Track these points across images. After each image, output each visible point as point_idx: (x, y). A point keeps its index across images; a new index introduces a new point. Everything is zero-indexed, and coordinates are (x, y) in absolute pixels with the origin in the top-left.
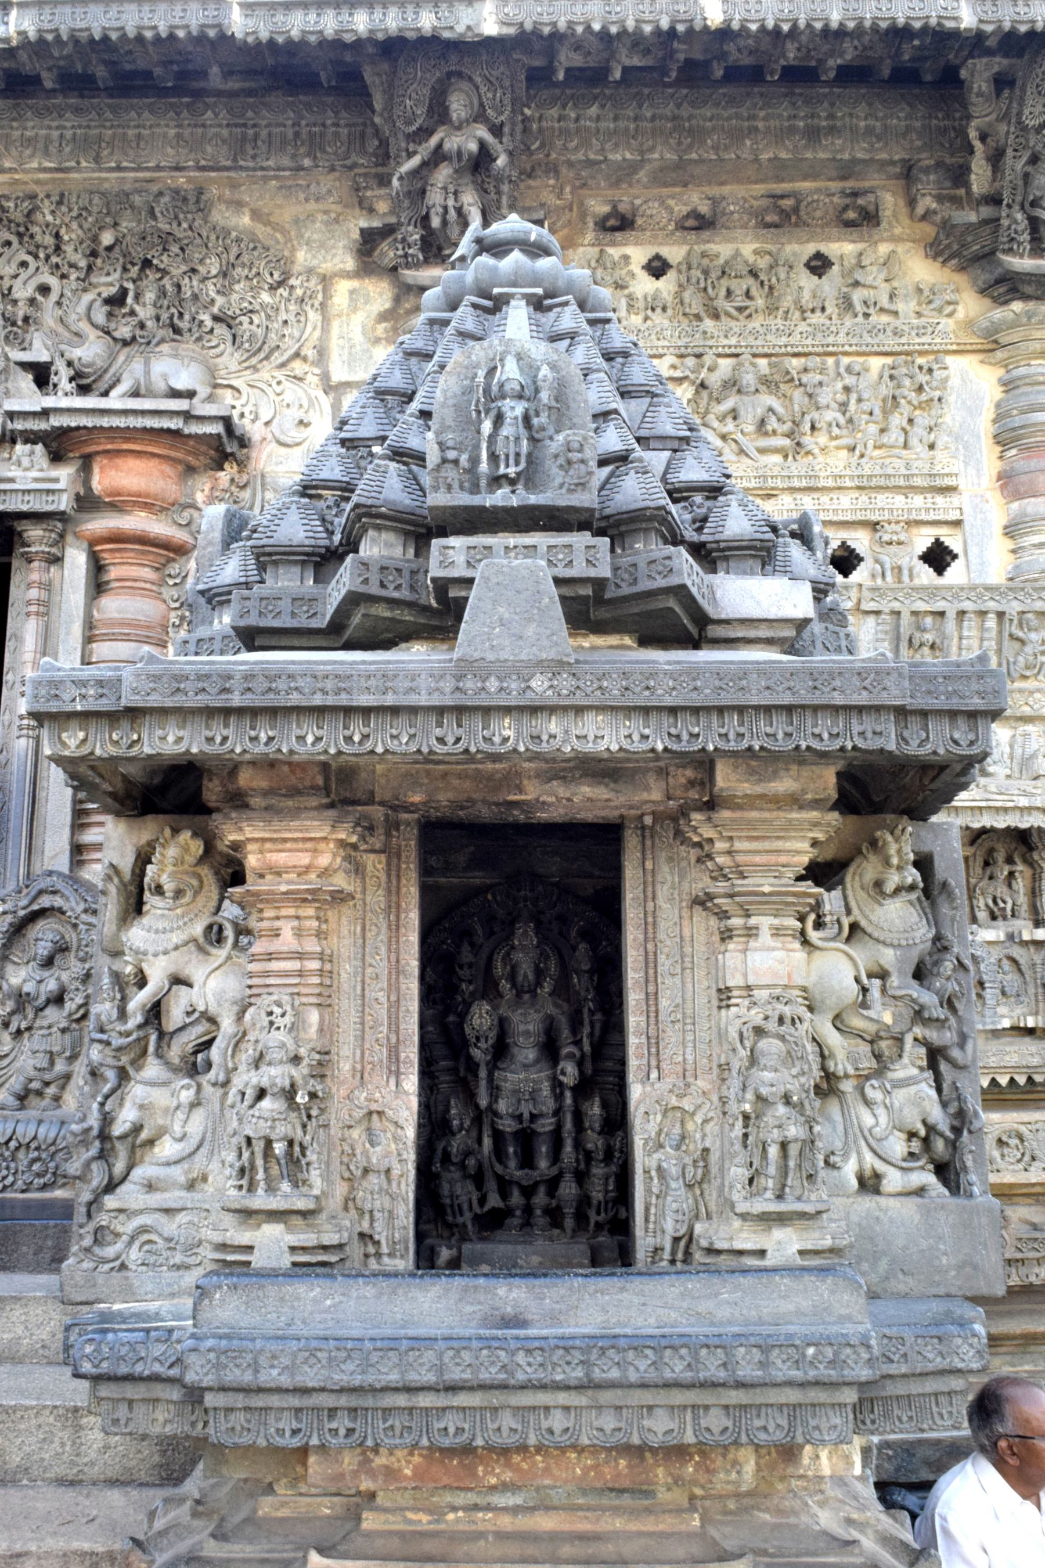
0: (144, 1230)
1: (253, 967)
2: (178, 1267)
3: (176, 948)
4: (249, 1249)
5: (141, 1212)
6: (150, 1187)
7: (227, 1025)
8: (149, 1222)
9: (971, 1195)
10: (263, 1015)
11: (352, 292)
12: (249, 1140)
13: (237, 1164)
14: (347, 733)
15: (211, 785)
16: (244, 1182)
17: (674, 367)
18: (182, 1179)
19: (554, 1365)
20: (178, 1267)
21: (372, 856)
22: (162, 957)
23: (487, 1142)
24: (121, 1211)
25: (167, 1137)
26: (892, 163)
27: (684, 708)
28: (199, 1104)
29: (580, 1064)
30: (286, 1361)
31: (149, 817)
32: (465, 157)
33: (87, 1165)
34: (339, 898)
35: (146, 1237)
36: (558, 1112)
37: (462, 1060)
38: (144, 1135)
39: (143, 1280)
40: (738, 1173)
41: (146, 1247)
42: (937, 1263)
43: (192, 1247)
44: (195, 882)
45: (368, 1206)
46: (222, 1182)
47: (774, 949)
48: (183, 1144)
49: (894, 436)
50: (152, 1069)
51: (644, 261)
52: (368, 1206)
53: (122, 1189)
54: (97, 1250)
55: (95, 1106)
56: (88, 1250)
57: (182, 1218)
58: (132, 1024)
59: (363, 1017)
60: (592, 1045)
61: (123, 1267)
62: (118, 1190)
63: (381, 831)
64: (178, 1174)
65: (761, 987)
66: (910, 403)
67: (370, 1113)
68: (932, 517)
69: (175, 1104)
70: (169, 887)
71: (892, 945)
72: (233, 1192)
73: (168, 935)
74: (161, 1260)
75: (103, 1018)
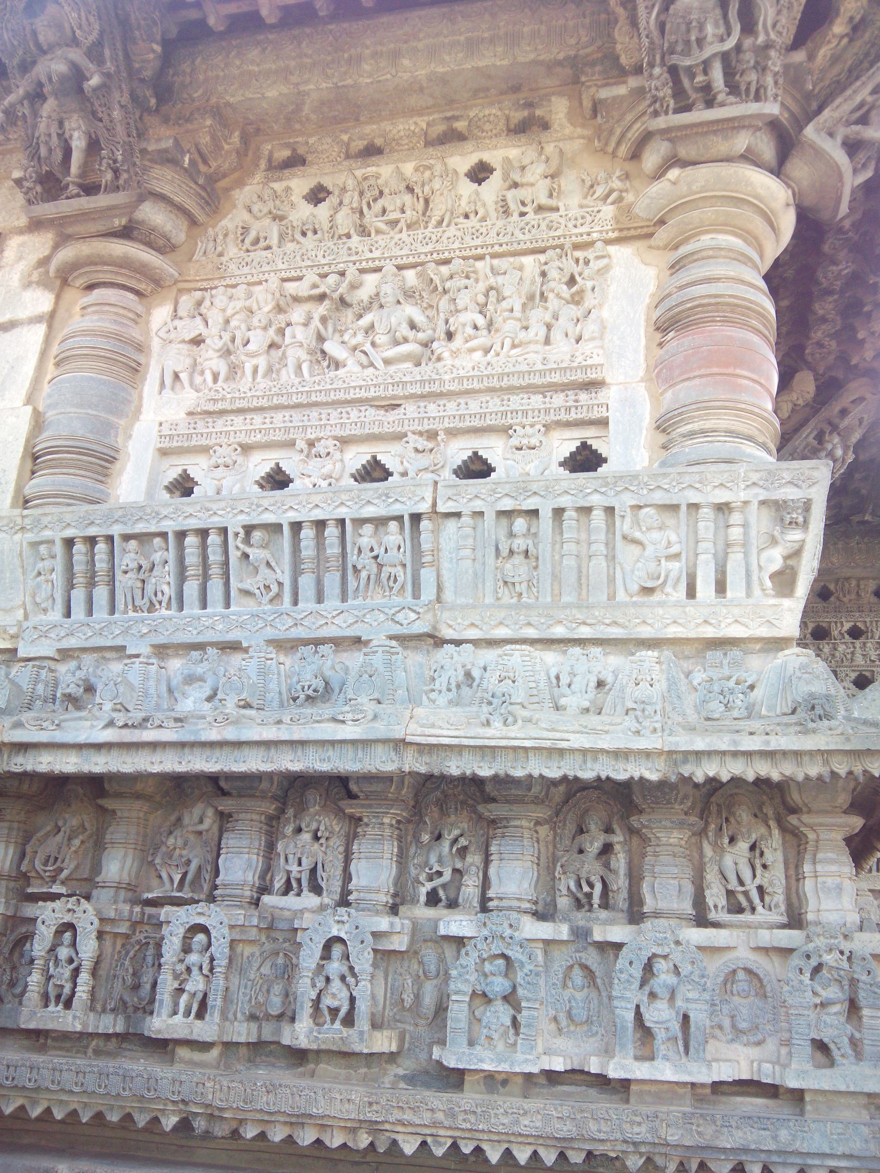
11: (22, 245)
17: (315, 286)
26: (559, 63)
32: (55, 79)
49: (537, 331)
51: (306, 191)
66: (558, 296)
68: (573, 416)
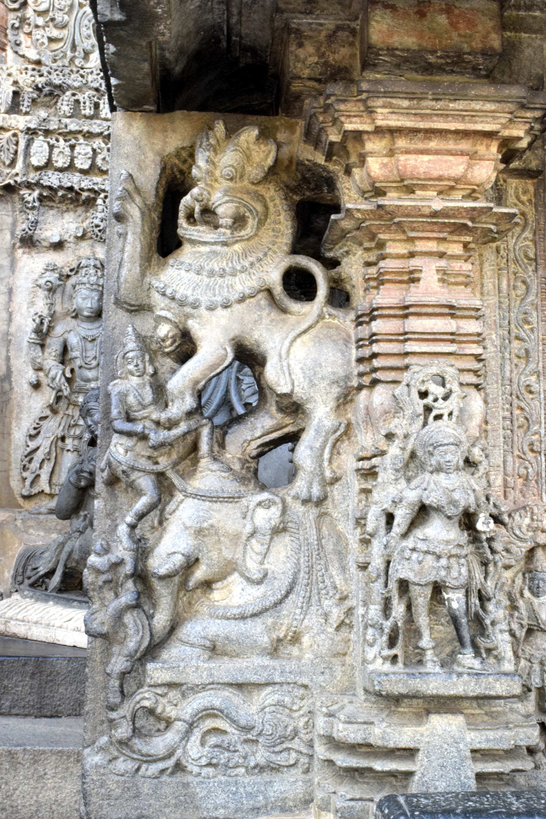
0: (210, 713)
2: (260, 769)
3: (242, 300)
4: (410, 753)
5: (204, 687)
6: (214, 650)
7: (321, 414)
8: (217, 703)
10: (415, 395)
12: (404, 586)
13: (388, 624)
15: (301, 53)
18: (265, 640)
20: (260, 769)
22: (220, 312)
24: (171, 685)
25: (235, 576)
28: (285, 530)
31: (178, 114)
33: (119, 617)
35: (209, 724)
38: (200, 573)
41: (213, 740)
43: (284, 738)
44: (259, 207)
48: (262, 588)
50: (209, 476)
53: (173, 652)
54: (137, 743)
55: (123, 529)
56: (123, 743)
57: (267, 697)
58: (176, 410)
61: (179, 767)
62: (165, 655)
64: (258, 631)
69: (248, 529)
70: (225, 210)
72: (380, 666)
73: (228, 280)
74: (236, 759)
75: (131, 399)
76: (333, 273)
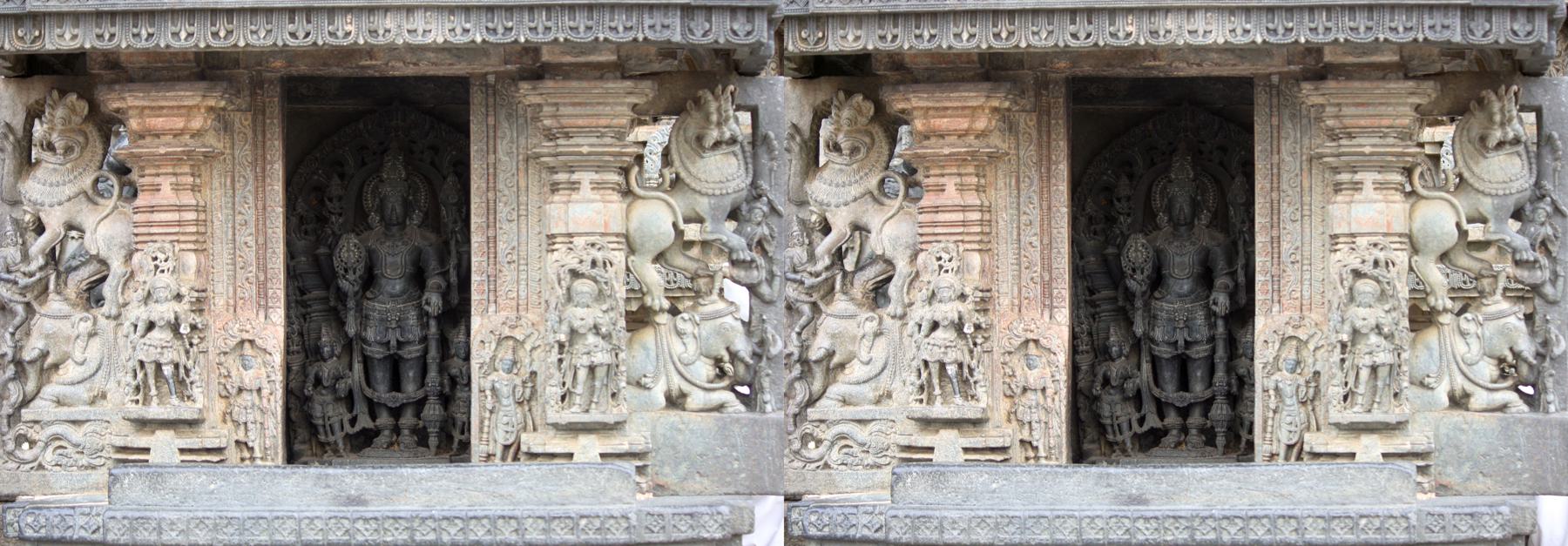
1: (138, 218)
3: (69, 199)
9: (763, 411)
14: (214, 29)
16: (140, 397)
19: (386, 530)
21: (239, 114)
23: (358, 366)
27: (500, 7)
29: (445, 296)
30: (182, 526)
34: (209, 157)
36: (424, 339)
37: (332, 290)
39: (58, 478)
40: (554, 391)
42: (729, 467)
45: (242, 419)
46: (120, 398)
47: (593, 201)
52: (242, 419)
59: (234, 259)
60: (458, 275)
63: (247, 93)
65: (580, 234)
67: (242, 342)
71: (707, 195)
76: (125, 178)
